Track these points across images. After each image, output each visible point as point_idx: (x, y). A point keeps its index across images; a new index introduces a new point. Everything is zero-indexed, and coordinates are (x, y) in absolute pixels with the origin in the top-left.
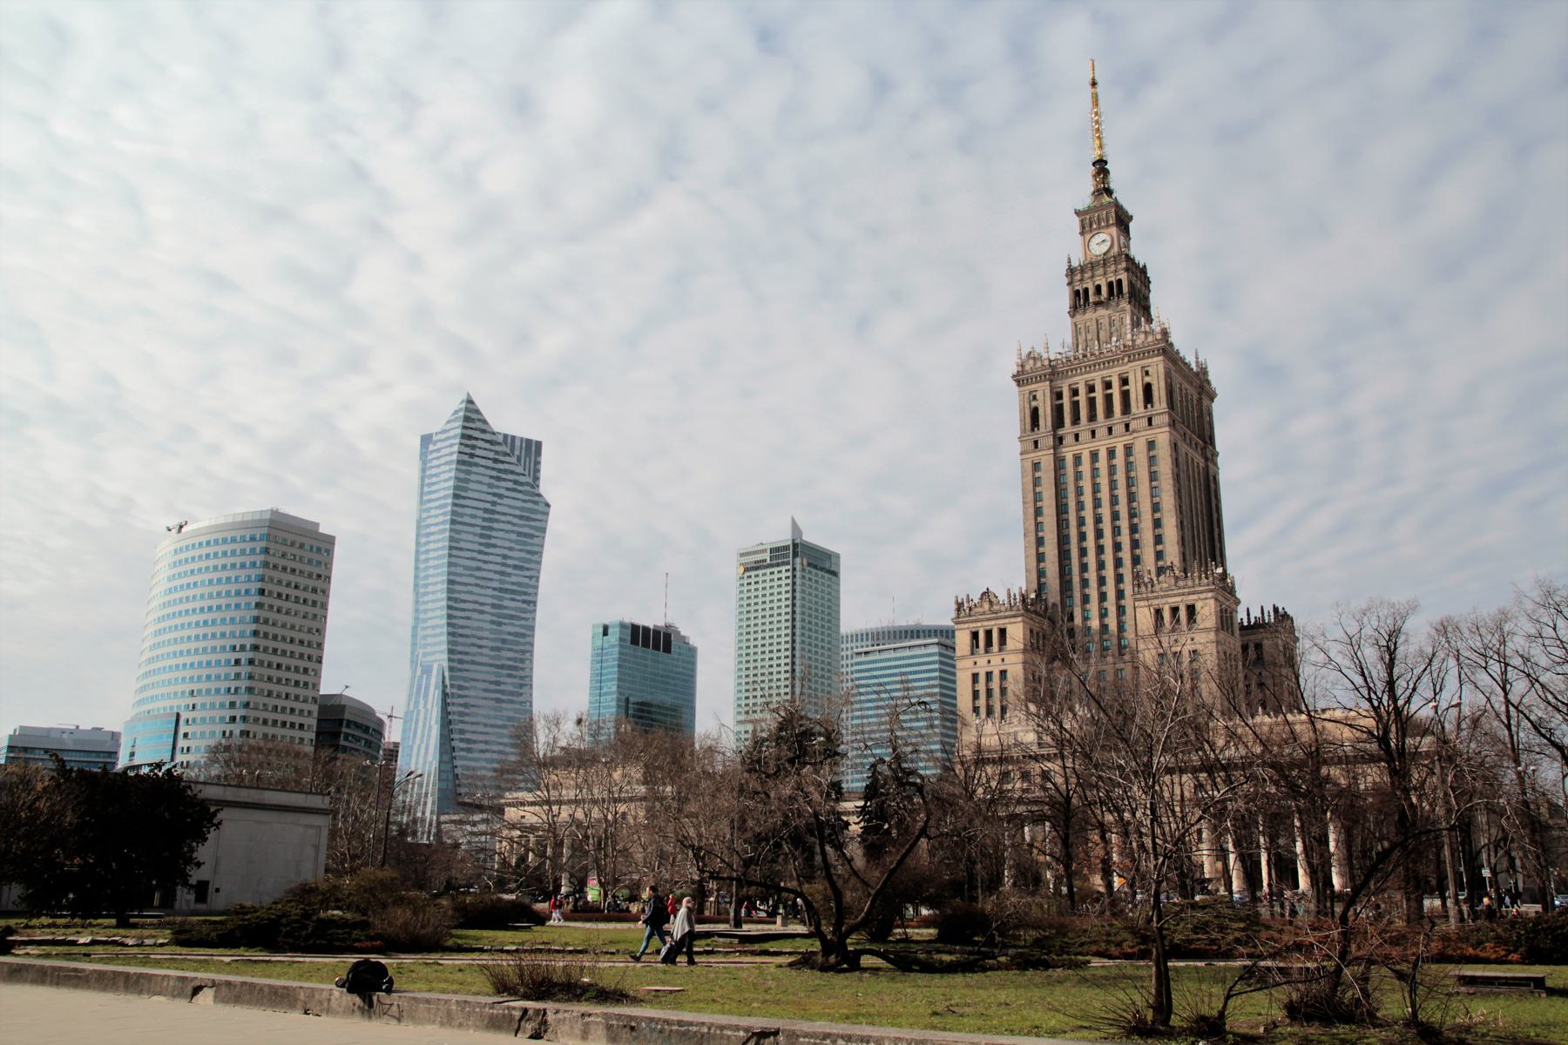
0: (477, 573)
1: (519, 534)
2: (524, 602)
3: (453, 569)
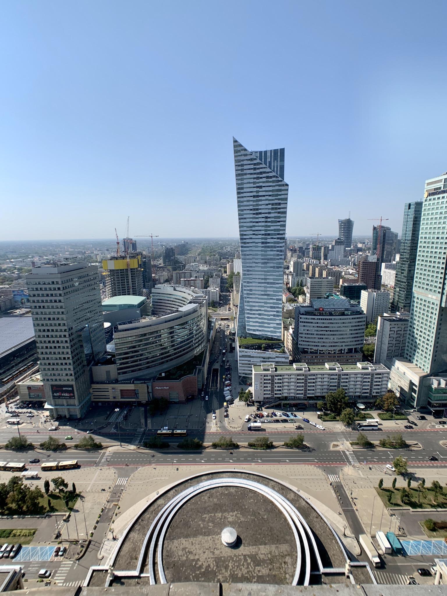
0: (253, 229)
1: (273, 204)
2: (278, 238)
3: (242, 229)
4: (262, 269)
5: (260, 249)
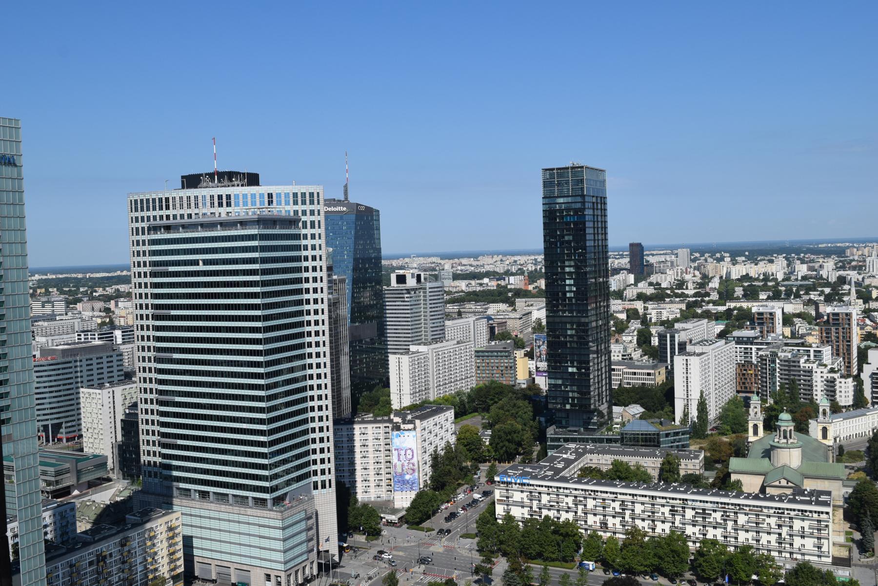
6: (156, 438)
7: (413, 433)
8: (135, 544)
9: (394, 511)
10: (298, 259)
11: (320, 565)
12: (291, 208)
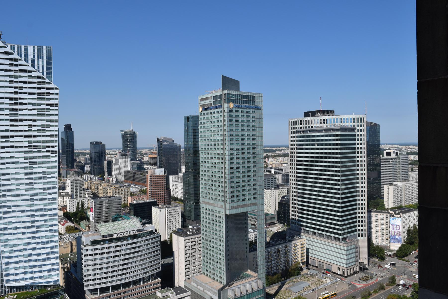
0: (11, 139)
2: (48, 152)
4: (27, 193)
5: (23, 165)
6: (296, 210)
7: (400, 219)
8: (289, 248)
9: (391, 251)
10: (354, 144)
11: (360, 268)
12: (352, 124)
